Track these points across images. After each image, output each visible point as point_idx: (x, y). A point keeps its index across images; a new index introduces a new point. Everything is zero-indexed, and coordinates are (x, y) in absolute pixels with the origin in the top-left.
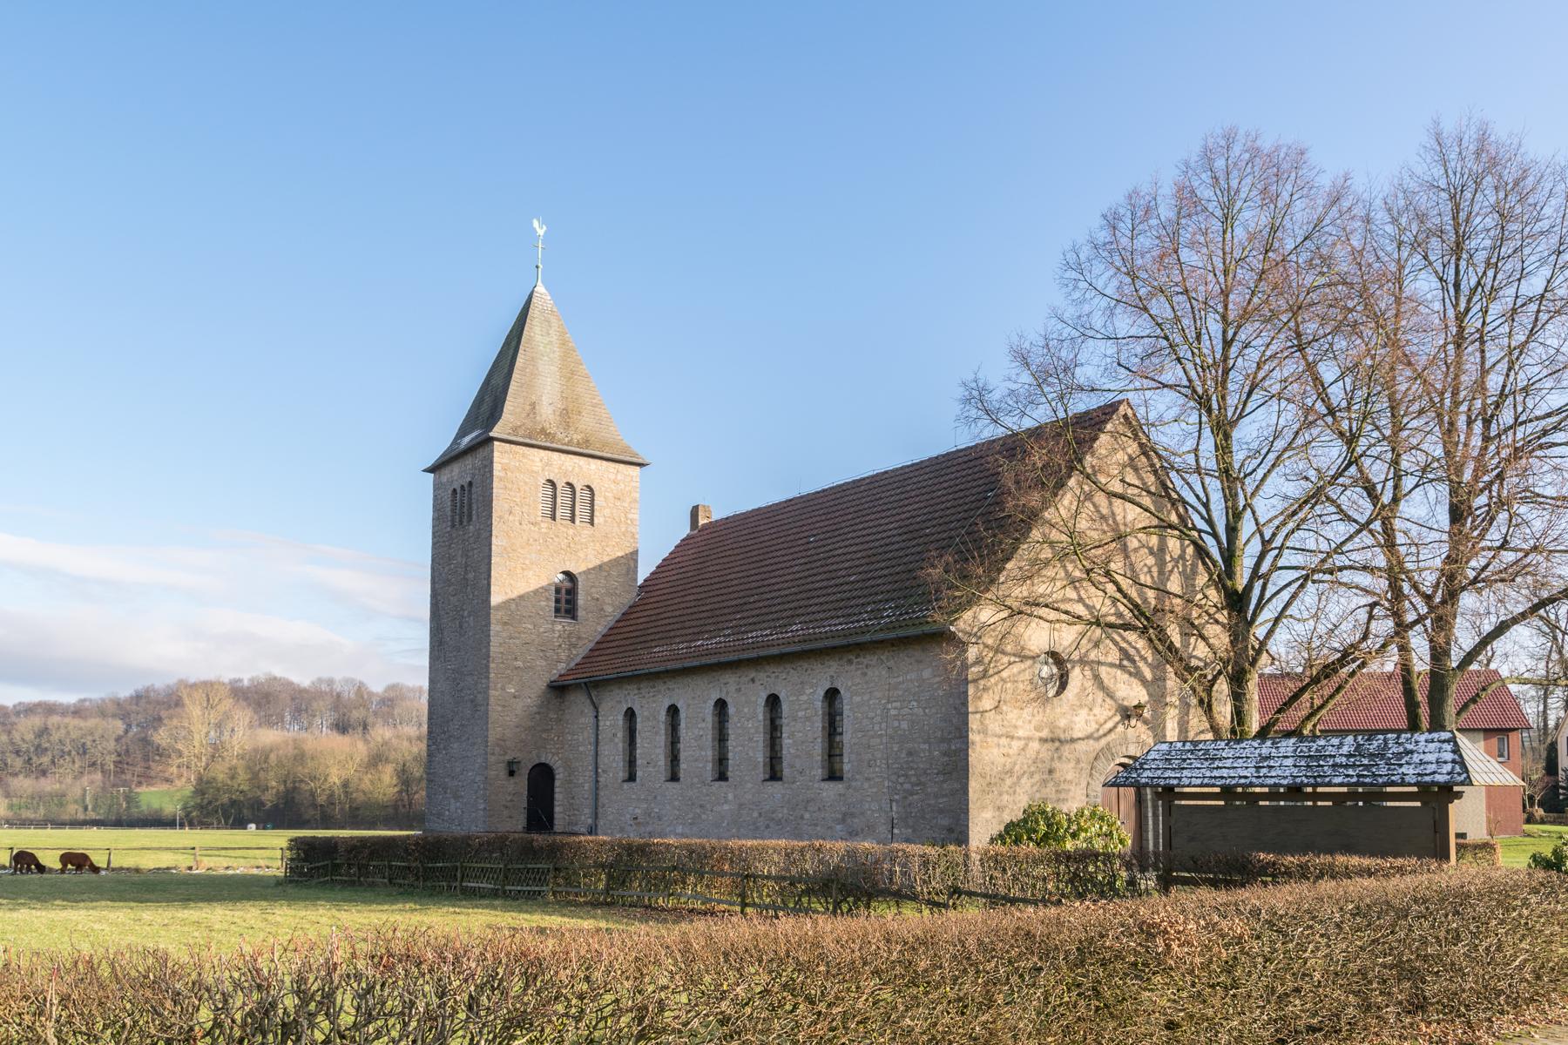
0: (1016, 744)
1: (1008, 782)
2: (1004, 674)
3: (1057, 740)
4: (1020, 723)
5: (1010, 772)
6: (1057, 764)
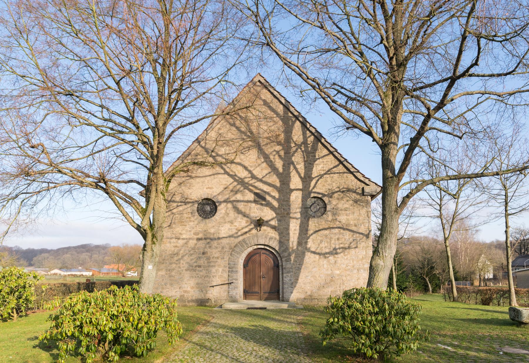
0: (181, 242)
1: (176, 258)
2: (174, 211)
3: (208, 239)
4: (184, 232)
5: (177, 254)
6: (208, 250)
